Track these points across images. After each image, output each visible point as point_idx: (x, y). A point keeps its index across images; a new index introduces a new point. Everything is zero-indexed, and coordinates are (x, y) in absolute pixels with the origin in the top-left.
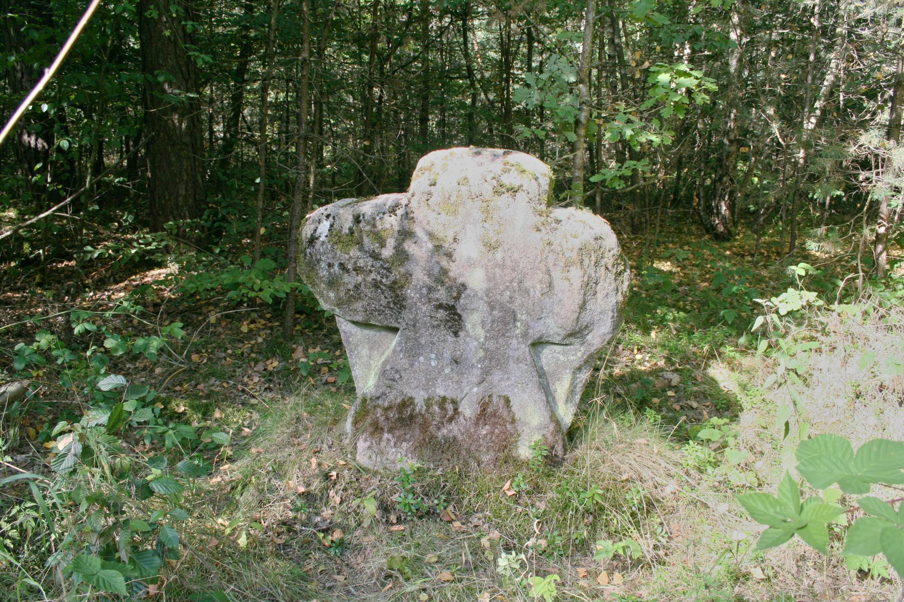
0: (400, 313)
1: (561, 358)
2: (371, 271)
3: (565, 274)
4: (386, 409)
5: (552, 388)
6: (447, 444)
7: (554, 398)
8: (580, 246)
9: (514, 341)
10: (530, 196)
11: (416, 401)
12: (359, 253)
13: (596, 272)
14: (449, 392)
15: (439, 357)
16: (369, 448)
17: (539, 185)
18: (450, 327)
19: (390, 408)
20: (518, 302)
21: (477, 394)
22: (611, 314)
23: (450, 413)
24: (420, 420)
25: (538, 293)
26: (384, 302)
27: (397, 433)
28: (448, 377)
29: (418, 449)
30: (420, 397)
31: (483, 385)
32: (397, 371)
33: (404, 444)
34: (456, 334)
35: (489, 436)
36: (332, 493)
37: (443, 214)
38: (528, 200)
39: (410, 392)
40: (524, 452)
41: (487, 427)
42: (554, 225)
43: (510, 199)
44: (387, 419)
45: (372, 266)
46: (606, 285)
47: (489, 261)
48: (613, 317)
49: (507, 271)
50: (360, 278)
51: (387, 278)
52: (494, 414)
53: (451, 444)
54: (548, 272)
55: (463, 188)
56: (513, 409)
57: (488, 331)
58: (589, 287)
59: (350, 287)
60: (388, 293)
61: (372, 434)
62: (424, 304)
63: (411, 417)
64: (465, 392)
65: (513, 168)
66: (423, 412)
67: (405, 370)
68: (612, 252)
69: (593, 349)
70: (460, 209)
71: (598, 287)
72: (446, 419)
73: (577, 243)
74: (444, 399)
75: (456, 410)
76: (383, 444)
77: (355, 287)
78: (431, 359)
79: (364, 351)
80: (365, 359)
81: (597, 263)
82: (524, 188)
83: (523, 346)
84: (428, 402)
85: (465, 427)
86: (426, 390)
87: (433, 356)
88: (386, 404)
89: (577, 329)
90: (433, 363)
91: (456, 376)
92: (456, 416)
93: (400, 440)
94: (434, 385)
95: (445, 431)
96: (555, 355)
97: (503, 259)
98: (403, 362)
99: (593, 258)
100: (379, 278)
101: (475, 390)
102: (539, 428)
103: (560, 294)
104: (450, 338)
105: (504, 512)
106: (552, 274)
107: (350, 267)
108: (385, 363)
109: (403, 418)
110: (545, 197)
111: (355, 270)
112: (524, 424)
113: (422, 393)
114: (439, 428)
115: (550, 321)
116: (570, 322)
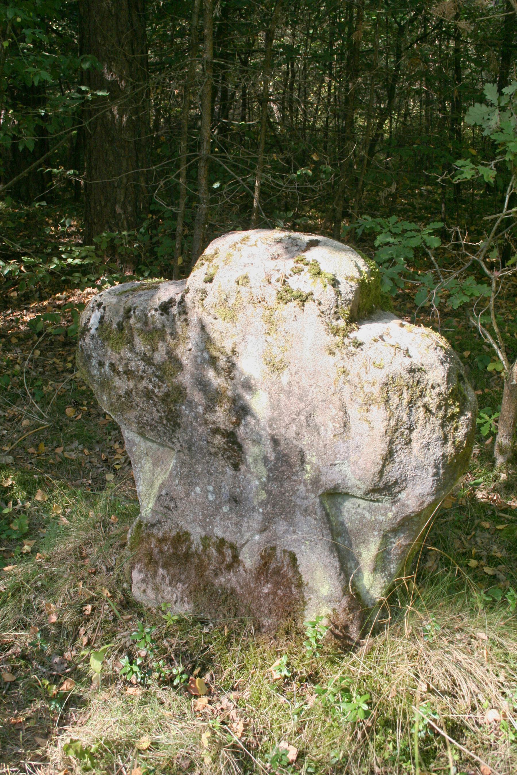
0: (174, 431)
1: (367, 515)
2: (142, 378)
3: (365, 414)
4: (162, 541)
5: (356, 551)
6: (223, 597)
7: (357, 564)
8: (384, 380)
9: (302, 488)
10: (322, 308)
11: (192, 538)
12: (130, 355)
13: (409, 415)
14: (228, 534)
16: (144, 581)
17: (338, 293)
18: (229, 458)
20: (306, 440)
21: (259, 543)
22: (432, 470)
23: (228, 560)
25: (330, 432)
26: (156, 416)
28: (225, 517)
29: (193, 594)
30: (197, 533)
31: (265, 534)
32: (172, 499)
33: (179, 585)
34: (236, 467)
35: (271, 597)
36: (82, 631)
37: (220, 319)
38: (319, 313)
41: (270, 585)
42: (352, 348)
43: (298, 309)
44: (161, 552)
45: (144, 372)
46: (427, 432)
47: (273, 384)
48: (436, 474)
49: (294, 400)
50: (131, 384)
51: (159, 388)
52: (277, 572)
54: (343, 408)
55: (243, 289)
56: (300, 569)
57: (270, 470)
59: (122, 392)
60: (161, 406)
62: (200, 425)
64: (245, 538)
65: (306, 268)
66: (200, 552)
67: (181, 499)
68: (437, 390)
69: (408, 511)
70: (240, 315)
71: (414, 435)
72: (223, 566)
73: (380, 376)
74: (222, 542)
75: (235, 557)
76: (158, 580)
77: (126, 393)
78: (208, 491)
79: (147, 465)
80: (148, 475)
81: (411, 403)
82: (315, 297)
83: (313, 496)
85: (244, 580)
86: (204, 527)
87: (211, 488)
88: (160, 535)
89: (381, 484)
90: (211, 497)
91: (235, 518)
92: (235, 565)
93: (174, 580)
94: (211, 523)
95: (223, 580)
96: (359, 510)
97: (290, 383)
98: (180, 490)
99: (406, 397)
100: (151, 387)
101: (257, 537)
103: (357, 439)
104: (229, 471)
105: (264, 697)
106: (349, 412)
109: (178, 556)
110: (346, 310)
111: (125, 372)
112: (312, 590)
113: (199, 529)
114: (216, 575)
115: (346, 469)
116: (369, 476)
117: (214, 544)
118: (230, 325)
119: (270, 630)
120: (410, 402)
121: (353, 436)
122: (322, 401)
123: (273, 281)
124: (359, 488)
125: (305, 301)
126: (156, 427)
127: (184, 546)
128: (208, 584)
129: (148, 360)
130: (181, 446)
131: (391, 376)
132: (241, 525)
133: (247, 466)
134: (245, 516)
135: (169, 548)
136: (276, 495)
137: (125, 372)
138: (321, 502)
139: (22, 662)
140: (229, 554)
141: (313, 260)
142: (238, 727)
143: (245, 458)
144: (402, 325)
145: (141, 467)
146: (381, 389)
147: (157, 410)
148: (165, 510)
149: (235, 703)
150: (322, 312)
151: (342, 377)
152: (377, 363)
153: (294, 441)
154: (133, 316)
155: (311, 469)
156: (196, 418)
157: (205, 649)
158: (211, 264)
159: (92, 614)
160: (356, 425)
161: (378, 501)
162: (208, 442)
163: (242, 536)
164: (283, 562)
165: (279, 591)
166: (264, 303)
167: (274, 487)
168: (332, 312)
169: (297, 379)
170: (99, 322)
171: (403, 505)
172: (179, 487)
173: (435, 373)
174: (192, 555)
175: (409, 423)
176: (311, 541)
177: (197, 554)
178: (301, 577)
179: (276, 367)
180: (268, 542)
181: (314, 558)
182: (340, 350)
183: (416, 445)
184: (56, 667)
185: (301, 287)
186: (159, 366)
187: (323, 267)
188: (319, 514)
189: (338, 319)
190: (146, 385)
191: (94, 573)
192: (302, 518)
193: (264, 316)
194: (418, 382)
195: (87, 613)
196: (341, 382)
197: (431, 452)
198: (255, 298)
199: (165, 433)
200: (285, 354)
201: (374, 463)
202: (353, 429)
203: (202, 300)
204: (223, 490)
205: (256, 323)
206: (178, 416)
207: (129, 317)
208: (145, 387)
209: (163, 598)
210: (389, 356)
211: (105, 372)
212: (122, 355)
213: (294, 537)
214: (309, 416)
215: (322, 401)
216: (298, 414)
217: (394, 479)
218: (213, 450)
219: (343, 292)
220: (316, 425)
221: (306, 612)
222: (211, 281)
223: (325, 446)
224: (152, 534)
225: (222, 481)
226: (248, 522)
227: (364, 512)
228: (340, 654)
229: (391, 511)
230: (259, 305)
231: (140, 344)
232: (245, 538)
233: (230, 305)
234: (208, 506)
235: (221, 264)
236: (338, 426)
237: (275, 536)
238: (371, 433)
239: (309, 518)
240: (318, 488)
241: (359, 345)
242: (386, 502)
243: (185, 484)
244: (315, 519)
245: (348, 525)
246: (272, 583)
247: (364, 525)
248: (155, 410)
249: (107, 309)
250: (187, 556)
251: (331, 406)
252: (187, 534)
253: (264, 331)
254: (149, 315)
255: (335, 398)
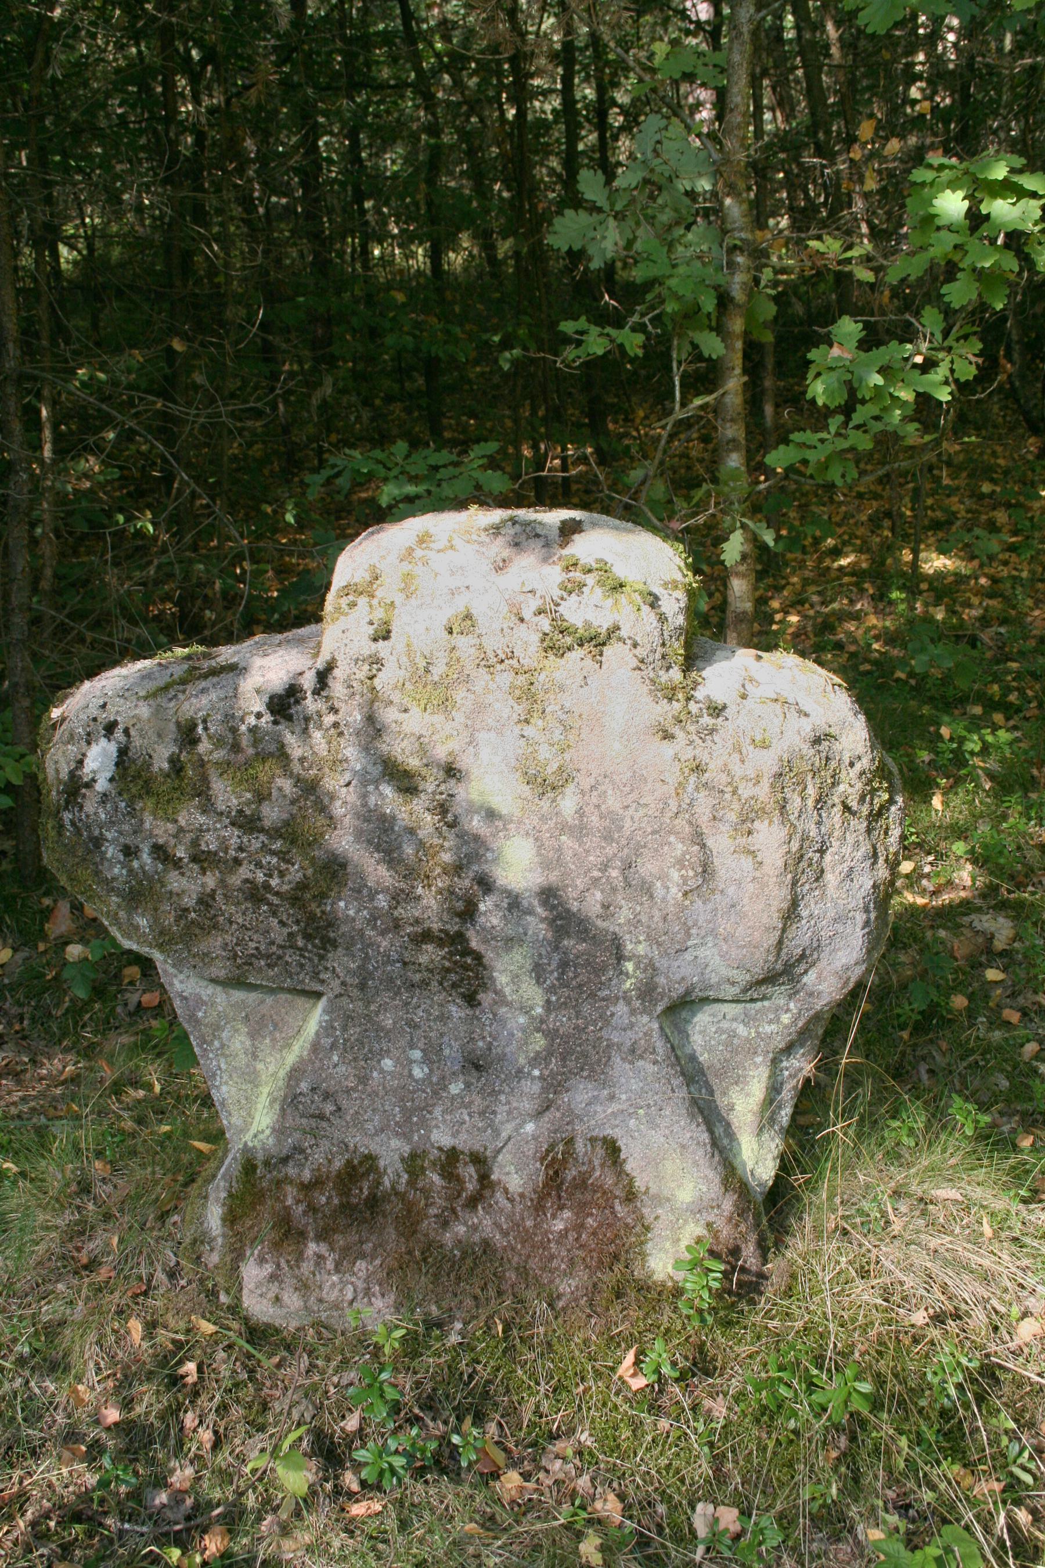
0: (322, 958)
1: (741, 1030)
2: (237, 862)
3: (742, 841)
4: (306, 1188)
5: (722, 1102)
6: (469, 1261)
7: (728, 1125)
8: (776, 769)
9: (621, 1008)
10: (640, 652)
11: (382, 1163)
12: (202, 819)
13: (819, 823)
14: (463, 1136)
15: (432, 1055)
16: (273, 1277)
17: (662, 618)
18: (454, 986)
19: (317, 1183)
20: (624, 915)
21: (535, 1138)
22: (860, 918)
23: (471, 1186)
24: (395, 1207)
25: (674, 890)
26: (279, 934)
27: (340, 1241)
29: (396, 1276)
30: (390, 1152)
31: (548, 1116)
32: (327, 1096)
33: (361, 1265)
34: (471, 1000)
35: (572, 1236)
36: (190, 1419)
37: (415, 711)
38: (635, 663)
39: (362, 1143)
40: (663, 1261)
41: (567, 1214)
42: (707, 720)
43: (588, 661)
45: (241, 849)
46: (847, 850)
47: (543, 819)
48: (867, 923)
49: (592, 841)
50: (210, 881)
51: (282, 874)
52: (582, 1183)
53: (480, 1255)
54: (698, 838)
55: (462, 642)
56: (628, 1167)
57: (551, 990)
58: (804, 865)
59: (189, 901)
60: (287, 912)
61: (277, 1245)
62: (383, 933)
63: (374, 1202)
64: (504, 1135)
65: (590, 579)
66: (402, 1188)
67: (348, 1091)
68: (858, 767)
69: (819, 1004)
70: (459, 694)
71: (828, 857)
72: (461, 1201)
73: (768, 762)
74: (452, 1155)
75: (484, 1178)
76: (306, 1267)
77: (201, 901)
78: (412, 1062)
79: (239, 1042)
80: (242, 1060)
81: (820, 802)
82: (624, 633)
83: (645, 1019)
84: (414, 1163)
85: (510, 1217)
86: (406, 1137)
87: (417, 1054)
88: (307, 1175)
89: (779, 967)
90: (418, 1073)
91: (478, 1100)
92: (487, 1193)
93: (346, 1258)
94: (423, 1123)
95: (461, 1229)
96: (725, 1025)
97: (580, 812)
98: (340, 1071)
99: (812, 791)
100: (260, 877)
101: (530, 1127)
102: (697, 1209)
103: (731, 890)
104: (457, 1011)
105: (626, 1433)
106: (710, 843)
107: (181, 853)
108: (295, 1074)
109: (352, 1205)
110: (678, 647)
111: (194, 859)
112: (659, 1200)
113: (395, 1143)
114: (445, 1224)
115: (709, 953)
116: (760, 956)
117: (434, 1163)
118: (438, 718)
119: (576, 1300)
120: (818, 801)
121: (722, 886)
122: (654, 832)
123: (527, 614)
124: (733, 984)
125: (604, 644)
126: (280, 958)
127: (366, 1185)
128: (429, 1246)
129: (247, 823)
130: (344, 984)
131: (785, 757)
132: (494, 1112)
133: (496, 992)
134: (500, 1092)
135: (329, 1198)
136: (569, 1036)
137: (194, 859)
138: (661, 1028)
139: (78, 1529)
140: (468, 1175)
141: (599, 561)
142: (609, 1506)
143: (491, 978)
144: (759, 658)
145: (223, 1046)
146: (772, 786)
147: (281, 922)
148: (313, 1122)
149: (577, 1461)
150: (642, 661)
151: (693, 779)
152: (758, 738)
153: (599, 923)
154: (204, 738)
155: (637, 967)
156: (373, 918)
157: (471, 1377)
158: (375, 602)
159: (201, 1379)
160: (729, 865)
161: (764, 998)
162: (405, 964)
163: (497, 1133)
164: (590, 1161)
165: (590, 1220)
166: (514, 662)
167: (562, 1021)
168: (658, 656)
169: (595, 800)
170: (117, 764)
171: (811, 994)
172: (342, 1069)
173: (851, 737)
174: (386, 1198)
175: (819, 839)
176: (649, 1106)
177: (397, 1194)
178: (631, 1181)
179: (546, 785)
180: (555, 1132)
181: (657, 1137)
182: (683, 729)
183: (831, 878)
184: (169, 1515)
185: (590, 617)
186: (277, 830)
187: (620, 571)
188: (660, 1050)
189: (668, 668)
190: (250, 876)
191: (145, 1294)
192: (627, 1066)
193: (513, 687)
194: (828, 759)
195: (190, 1380)
196: (690, 788)
197: (856, 885)
198: (490, 654)
199: (302, 966)
200: (567, 756)
201: (767, 929)
202: (722, 873)
203: (371, 678)
204: (447, 1052)
205: (497, 706)
206: (330, 925)
207: (195, 741)
208: (247, 881)
209: (321, 1301)
210: (776, 721)
211: (142, 867)
212: (182, 822)
213: (614, 1107)
214: (628, 866)
215: (654, 832)
216: (605, 867)
217: (799, 951)
218: (417, 977)
219: (669, 615)
220: (644, 883)
221: (650, 1245)
222: (384, 634)
223: (665, 919)
224: (286, 1177)
225: (442, 1035)
226: (508, 1103)
227: (735, 1025)
228: (733, 1304)
229: (788, 1010)
230: (499, 667)
231: (226, 794)
232: (504, 1135)
233: (436, 678)
234: (414, 1092)
235: (399, 599)
236: (691, 873)
237: (571, 1116)
238: (758, 874)
239: (641, 1063)
240: (654, 1002)
241: (717, 710)
242: (779, 995)
243: (355, 1059)
244: (655, 1062)
245: (703, 1058)
246: (571, 1208)
247: (735, 1052)
248: (274, 922)
249: (132, 732)
250: (374, 1202)
251: (672, 839)
252: (370, 1159)
253: (515, 717)
254: (243, 728)
255: (681, 823)
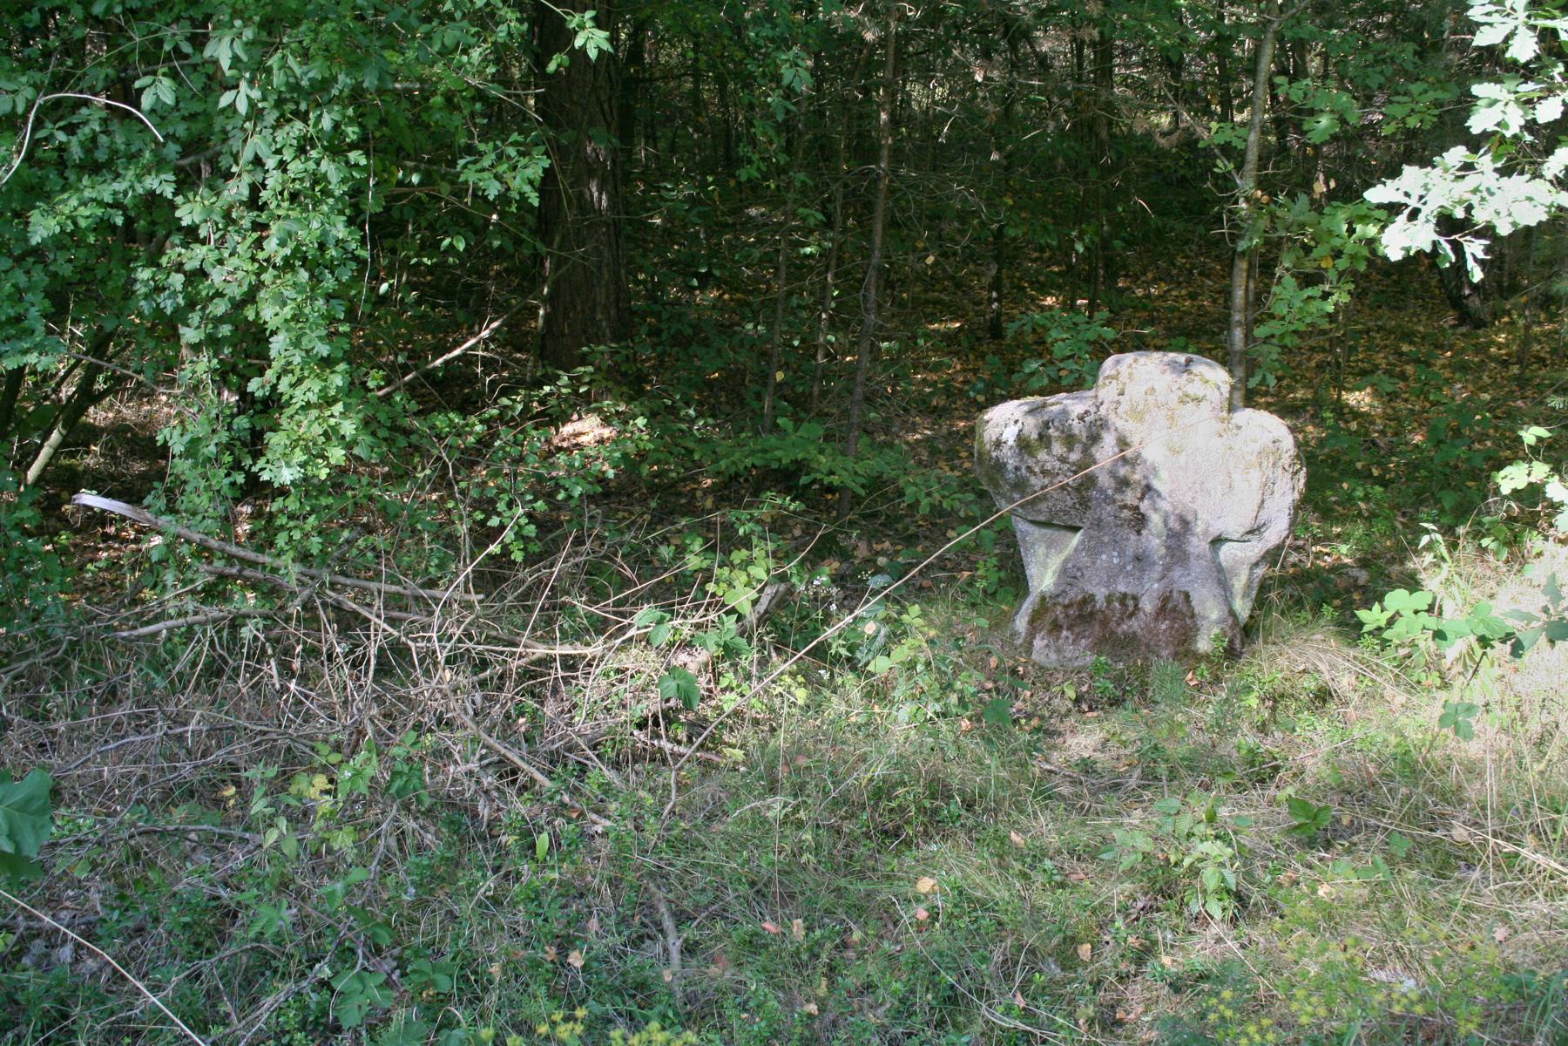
4: (1066, 607)
15: (1121, 554)
19: (1070, 605)
24: (1100, 616)
26: (1070, 503)
27: (1076, 630)
28: (1129, 574)
29: (1098, 646)
30: (1100, 593)
39: (1090, 589)
40: (1203, 645)
44: (1067, 616)
52: (1174, 610)
53: (1131, 641)
58: (1268, 486)
60: (1074, 494)
61: (1050, 632)
63: (1092, 614)
70: (1147, 417)
73: (1256, 447)
74: (1125, 595)
75: (1136, 606)
79: (1041, 550)
84: (1109, 599)
98: (1084, 559)
102: (1219, 622)
104: (1133, 537)
107: (1037, 470)
108: (1066, 561)
112: (1204, 618)
128: (1112, 633)
140: (1129, 605)
181: (1205, 591)
222: (1122, 394)
237: (1172, 581)
241: (1239, 428)
252: (1093, 595)
